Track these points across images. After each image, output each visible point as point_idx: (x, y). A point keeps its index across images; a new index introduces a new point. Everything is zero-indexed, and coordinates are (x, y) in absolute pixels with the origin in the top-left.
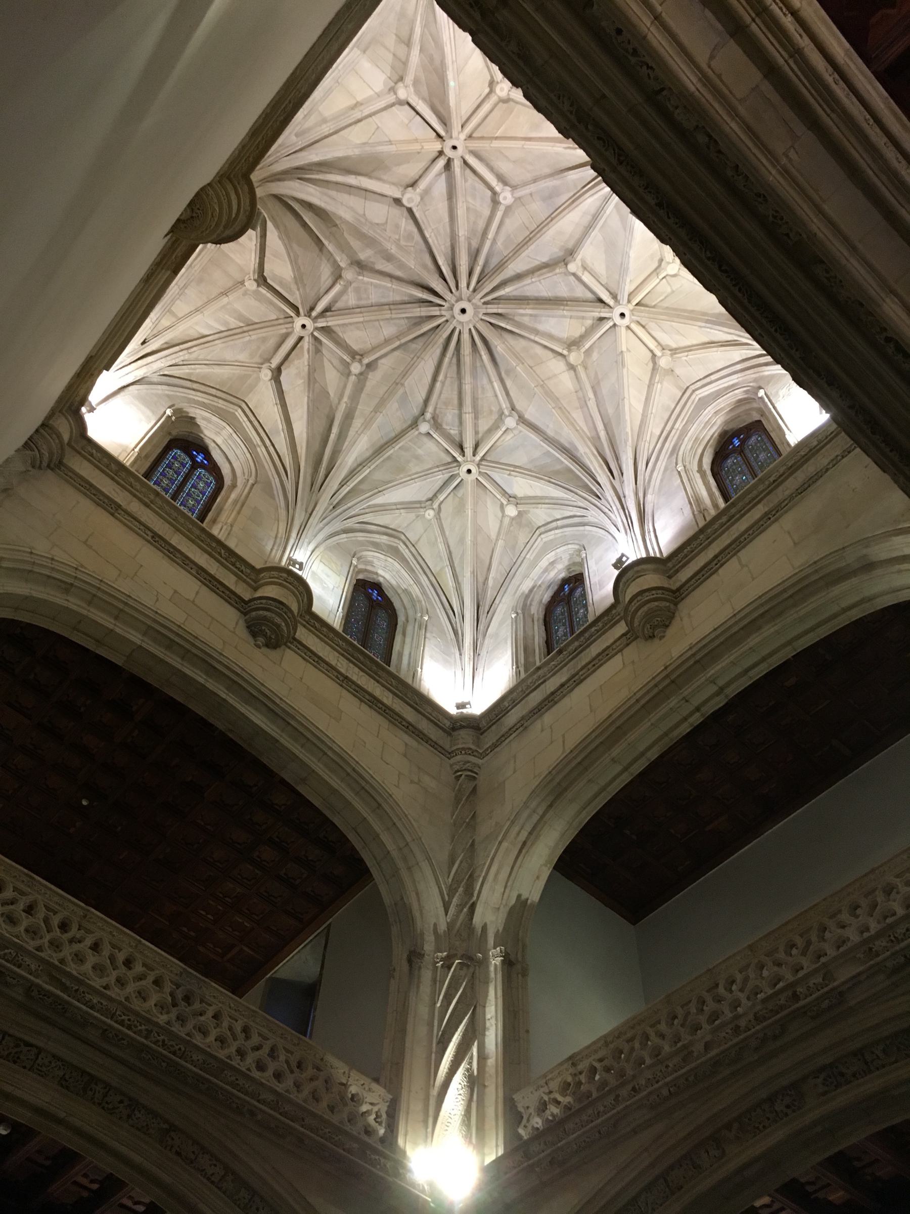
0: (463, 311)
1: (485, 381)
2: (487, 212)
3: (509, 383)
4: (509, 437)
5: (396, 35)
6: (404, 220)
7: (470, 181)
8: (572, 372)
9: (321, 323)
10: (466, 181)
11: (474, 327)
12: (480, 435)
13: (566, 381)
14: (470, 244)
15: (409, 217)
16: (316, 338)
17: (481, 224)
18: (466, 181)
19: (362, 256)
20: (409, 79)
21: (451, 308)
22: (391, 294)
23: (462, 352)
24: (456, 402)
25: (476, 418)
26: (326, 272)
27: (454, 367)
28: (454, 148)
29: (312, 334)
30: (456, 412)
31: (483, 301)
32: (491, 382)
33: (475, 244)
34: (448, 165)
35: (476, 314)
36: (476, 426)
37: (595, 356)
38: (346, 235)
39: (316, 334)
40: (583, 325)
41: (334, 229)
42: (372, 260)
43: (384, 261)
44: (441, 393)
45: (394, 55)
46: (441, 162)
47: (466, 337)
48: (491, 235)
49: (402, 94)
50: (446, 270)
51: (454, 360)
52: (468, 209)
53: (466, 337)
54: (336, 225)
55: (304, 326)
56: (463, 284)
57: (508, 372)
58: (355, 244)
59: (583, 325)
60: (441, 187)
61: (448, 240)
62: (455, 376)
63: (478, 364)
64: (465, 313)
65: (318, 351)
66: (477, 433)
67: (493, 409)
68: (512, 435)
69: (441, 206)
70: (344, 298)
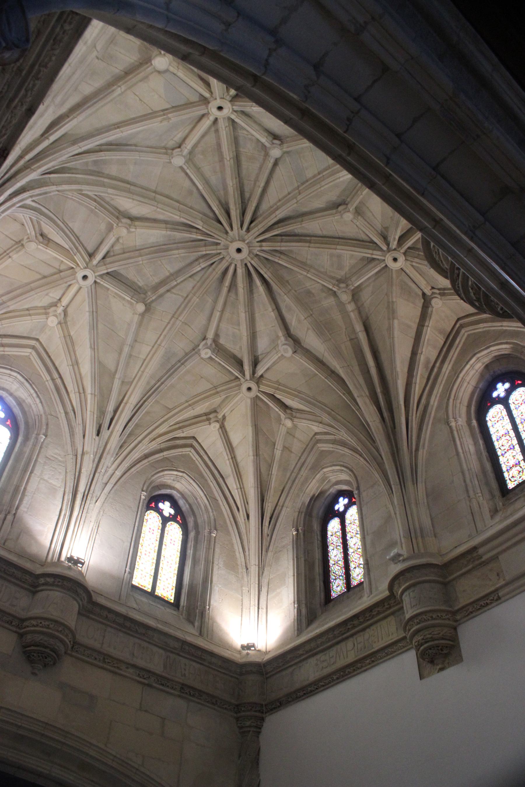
0: (239, 251)
1: (214, 180)
2: (223, 325)
3: (187, 183)
4: (179, 136)
5: (291, 452)
6: (293, 324)
7: (238, 348)
8: (121, 209)
9: (377, 255)
10: (241, 348)
11: (227, 233)
12: (213, 129)
13: (127, 204)
14: (237, 294)
15: (289, 326)
16: (385, 238)
17: (227, 315)
18: (241, 348)
19: (331, 301)
20: (283, 430)
21: (250, 252)
22: (309, 257)
23: (239, 206)
24: (243, 159)
25: (219, 145)
26: (366, 297)
27: (247, 189)
28: (249, 389)
29: (389, 250)
30: (241, 149)
31: (222, 256)
32: (207, 182)
33: (232, 295)
34: (255, 363)
35: (227, 248)
36: (218, 138)
37: (103, 227)
38: (344, 327)
39: (385, 248)
40: (123, 244)
41: (353, 337)
42: (324, 294)
43: (313, 291)
44: (261, 168)
45: (294, 437)
46: (260, 371)
47: (236, 224)
48: (217, 314)
49: (289, 423)
50: (258, 282)
51: (247, 195)
52: (239, 325)
53: (236, 224)
54: (351, 340)
55: (395, 260)
56: (240, 271)
57: (190, 193)
58: (337, 316)
59: (123, 244)
60: (262, 344)
61: (256, 298)
62: (246, 182)
63: (222, 193)
64: (238, 248)
65: (386, 229)
66: (217, 131)
67: (201, 157)
68: (175, 139)
69: (260, 326)
70: (353, 262)
